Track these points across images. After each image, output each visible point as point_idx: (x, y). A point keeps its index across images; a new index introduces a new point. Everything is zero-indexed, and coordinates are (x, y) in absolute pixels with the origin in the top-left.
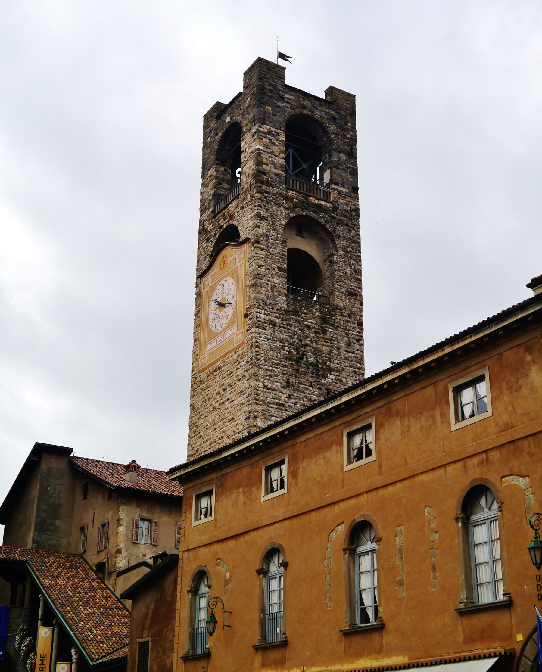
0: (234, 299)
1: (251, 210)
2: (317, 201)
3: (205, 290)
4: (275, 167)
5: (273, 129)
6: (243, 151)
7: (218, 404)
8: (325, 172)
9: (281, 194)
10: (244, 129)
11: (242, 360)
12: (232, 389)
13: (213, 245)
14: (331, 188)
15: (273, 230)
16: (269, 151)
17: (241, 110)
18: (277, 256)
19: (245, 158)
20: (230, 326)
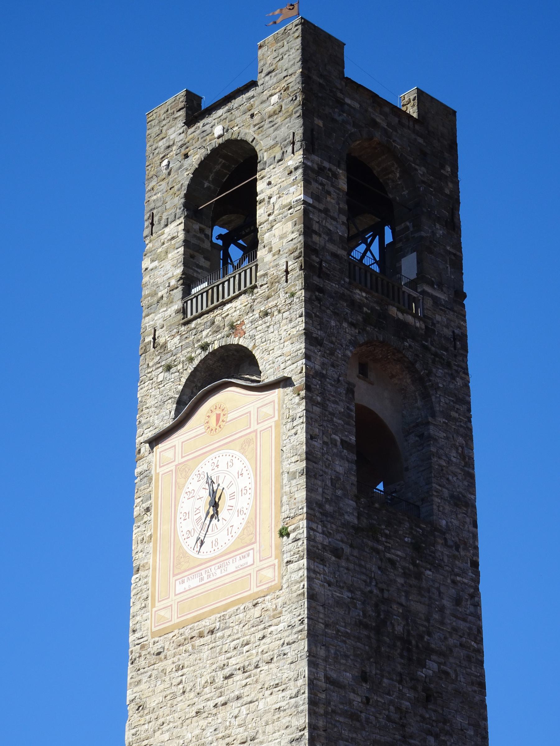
0: (248, 496)
1: (291, 321)
2: (400, 316)
3: (165, 469)
4: (331, 240)
5: (326, 164)
7: (211, 704)
8: (404, 256)
9: (343, 294)
10: (264, 156)
11: (276, 621)
12: (249, 676)
13: (184, 380)
14: (419, 290)
15: (333, 366)
16: (321, 207)
17: (252, 116)
18: (340, 419)
19: (269, 215)
20: (238, 549)
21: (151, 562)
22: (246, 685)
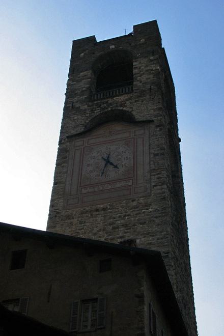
12: (130, 229)
13: (89, 119)
22: (127, 232)
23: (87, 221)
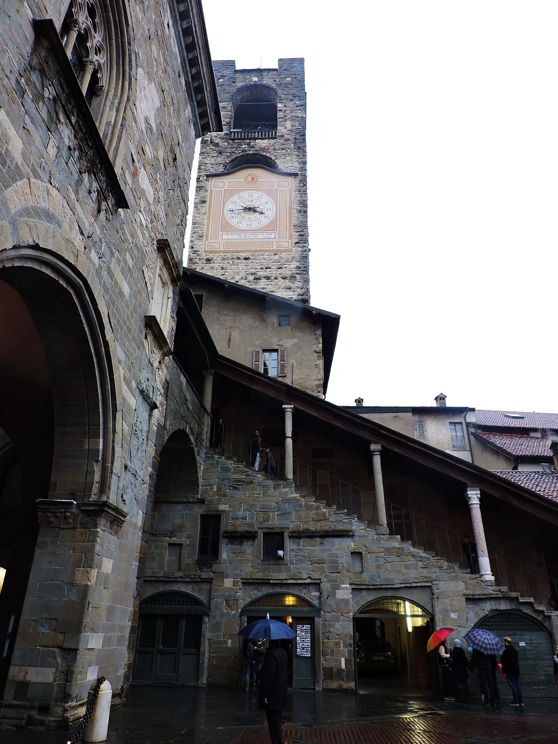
3: (217, 189)
6: (280, 110)
12: (272, 281)
19: (285, 116)
20: (265, 231)
21: (206, 222)
23: (228, 268)
